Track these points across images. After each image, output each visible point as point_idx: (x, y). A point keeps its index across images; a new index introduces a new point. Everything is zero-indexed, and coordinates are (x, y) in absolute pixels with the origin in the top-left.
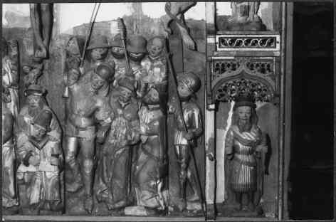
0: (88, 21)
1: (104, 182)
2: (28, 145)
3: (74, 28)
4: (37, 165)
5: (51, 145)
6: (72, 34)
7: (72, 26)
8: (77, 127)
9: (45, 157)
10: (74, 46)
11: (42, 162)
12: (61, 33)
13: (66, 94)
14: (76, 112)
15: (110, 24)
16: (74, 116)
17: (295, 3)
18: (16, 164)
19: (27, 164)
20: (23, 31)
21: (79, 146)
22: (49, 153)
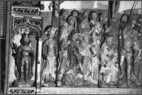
0: (131, 8)
1: (134, 74)
2: (107, 59)
3: (124, 11)
4: (110, 67)
5: (115, 60)
6: (123, 13)
7: (123, 10)
8: (127, 51)
9: (112, 64)
10: (125, 19)
11: (112, 66)
12: (119, 12)
13: (120, 38)
14: (127, 45)
15: (138, 10)
16: (125, 47)
17: (109, 1)
18: (100, 67)
19: (105, 66)
20: (105, 11)
21: (126, 60)
22: (114, 63)
